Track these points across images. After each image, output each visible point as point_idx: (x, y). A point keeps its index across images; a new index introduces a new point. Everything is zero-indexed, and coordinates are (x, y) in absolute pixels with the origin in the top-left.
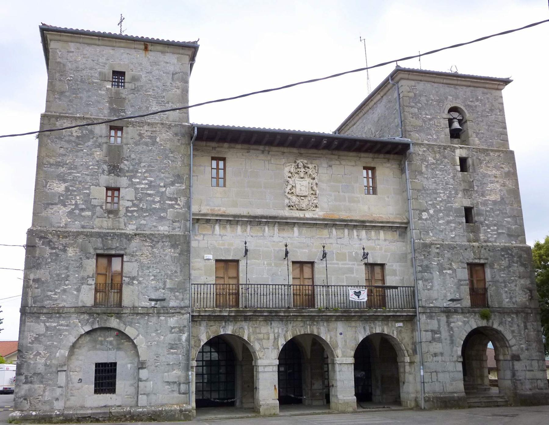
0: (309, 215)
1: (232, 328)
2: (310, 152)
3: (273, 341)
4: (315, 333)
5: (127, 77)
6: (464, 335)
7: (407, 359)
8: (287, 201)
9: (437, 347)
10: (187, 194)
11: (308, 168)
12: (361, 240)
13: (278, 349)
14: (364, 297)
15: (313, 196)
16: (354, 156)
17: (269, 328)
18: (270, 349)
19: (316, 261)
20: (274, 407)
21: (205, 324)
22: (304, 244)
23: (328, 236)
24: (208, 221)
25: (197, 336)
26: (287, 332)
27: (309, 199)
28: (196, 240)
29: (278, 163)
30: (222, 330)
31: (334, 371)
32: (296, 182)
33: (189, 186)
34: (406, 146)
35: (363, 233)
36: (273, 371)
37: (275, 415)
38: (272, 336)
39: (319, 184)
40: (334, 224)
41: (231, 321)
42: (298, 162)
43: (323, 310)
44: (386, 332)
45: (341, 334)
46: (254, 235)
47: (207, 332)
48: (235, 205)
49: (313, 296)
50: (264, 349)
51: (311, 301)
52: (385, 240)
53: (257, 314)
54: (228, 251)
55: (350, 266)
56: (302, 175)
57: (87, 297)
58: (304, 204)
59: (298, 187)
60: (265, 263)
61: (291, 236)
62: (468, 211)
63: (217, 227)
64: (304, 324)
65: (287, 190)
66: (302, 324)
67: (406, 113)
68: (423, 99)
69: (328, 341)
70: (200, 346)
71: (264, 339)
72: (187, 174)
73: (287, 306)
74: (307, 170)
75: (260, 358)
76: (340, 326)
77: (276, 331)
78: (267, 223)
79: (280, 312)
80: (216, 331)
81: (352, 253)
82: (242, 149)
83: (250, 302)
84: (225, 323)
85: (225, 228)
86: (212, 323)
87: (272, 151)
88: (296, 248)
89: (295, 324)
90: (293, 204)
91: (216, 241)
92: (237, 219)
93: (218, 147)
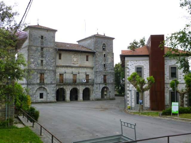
0: (76, 65)
5: (44, 37)
6: (102, 88)
7: (92, 92)
8: (72, 63)
9: (97, 90)
10: (55, 62)
14: (85, 81)
22: (75, 71)
31: (79, 94)
33: (55, 60)
34: (95, 52)
57: (38, 81)
58: (75, 63)
62: (104, 65)
63: (60, 68)
68: (98, 42)
76: (81, 86)
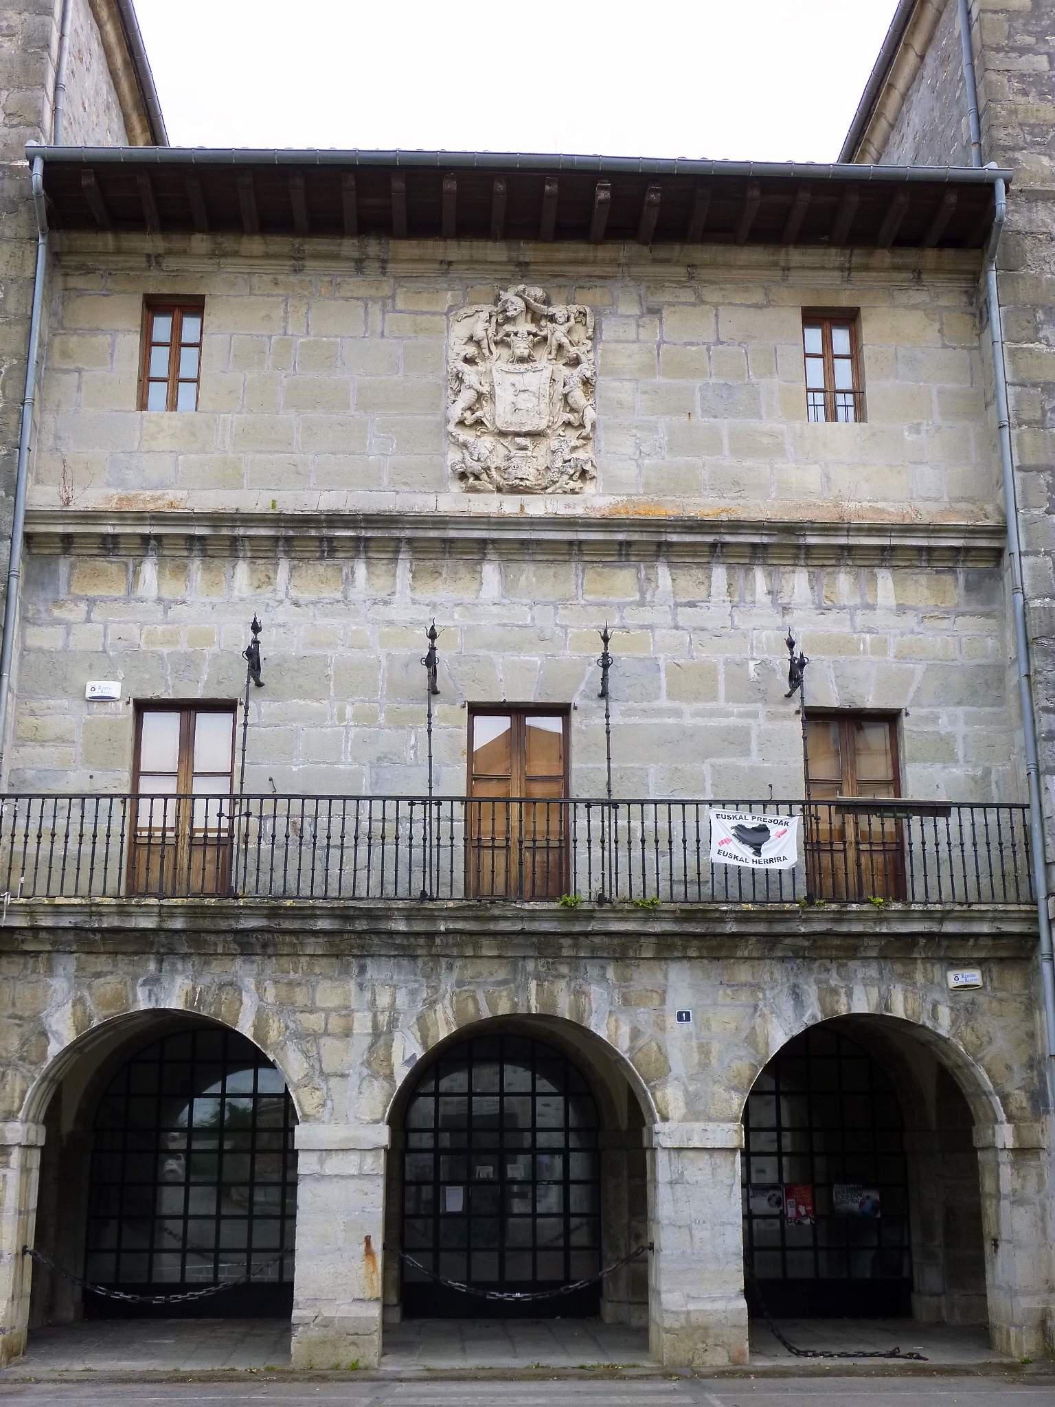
1: (188, 984)
2: (562, 256)
3: (367, 1041)
4: (564, 1009)
7: (1005, 1135)
8: (454, 456)
11: (552, 318)
12: (786, 609)
13: (390, 1077)
15: (572, 436)
16: (759, 267)
17: (352, 986)
18: (354, 1079)
19: (576, 700)
20: (355, 1335)
21: (71, 968)
22: (515, 631)
23: (637, 597)
24: (109, 544)
25: (36, 1018)
26: (431, 1004)
27: (554, 444)
28: (59, 622)
29: (426, 308)
30: (141, 993)
32: (497, 377)
35: (798, 582)
36: (361, 1176)
37: (355, 1373)
38: (362, 1024)
39: (601, 382)
40: (659, 544)
41: (185, 957)
42: (505, 296)
43: (586, 906)
44: (899, 1011)
45: (683, 1017)
46: (305, 596)
47: (79, 1001)
48: (232, 480)
49: (561, 852)
50: (325, 1076)
51: (556, 876)
52: (901, 609)
53: (287, 925)
54: (189, 662)
55: (732, 721)
56: (521, 347)
58: (528, 468)
59: (504, 395)
60: (349, 710)
61: (468, 597)
63: (149, 569)
64: (515, 970)
65: (456, 412)
66: (502, 974)
67: (993, 77)
69: (622, 1046)
70: (43, 1056)
71: (326, 1033)
72: (15, 355)
73: (416, 893)
74: (547, 328)
75: (306, 1117)
76: (681, 984)
77: (384, 1000)
78: (361, 547)
79: (387, 914)
80: (118, 998)
81: (742, 665)
82: (267, 256)
83: (278, 874)
84: (160, 962)
85: (181, 570)
86: (101, 963)
87: (396, 260)
88: (489, 646)
89: (469, 973)
90: (477, 467)
91: (142, 625)
92: (225, 532)
93: (169, 252)
